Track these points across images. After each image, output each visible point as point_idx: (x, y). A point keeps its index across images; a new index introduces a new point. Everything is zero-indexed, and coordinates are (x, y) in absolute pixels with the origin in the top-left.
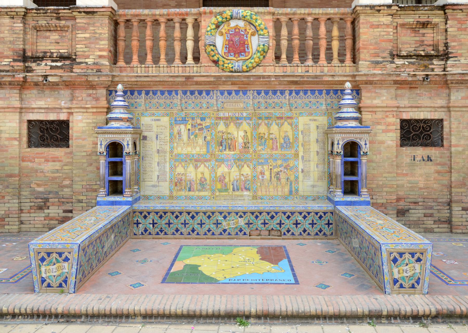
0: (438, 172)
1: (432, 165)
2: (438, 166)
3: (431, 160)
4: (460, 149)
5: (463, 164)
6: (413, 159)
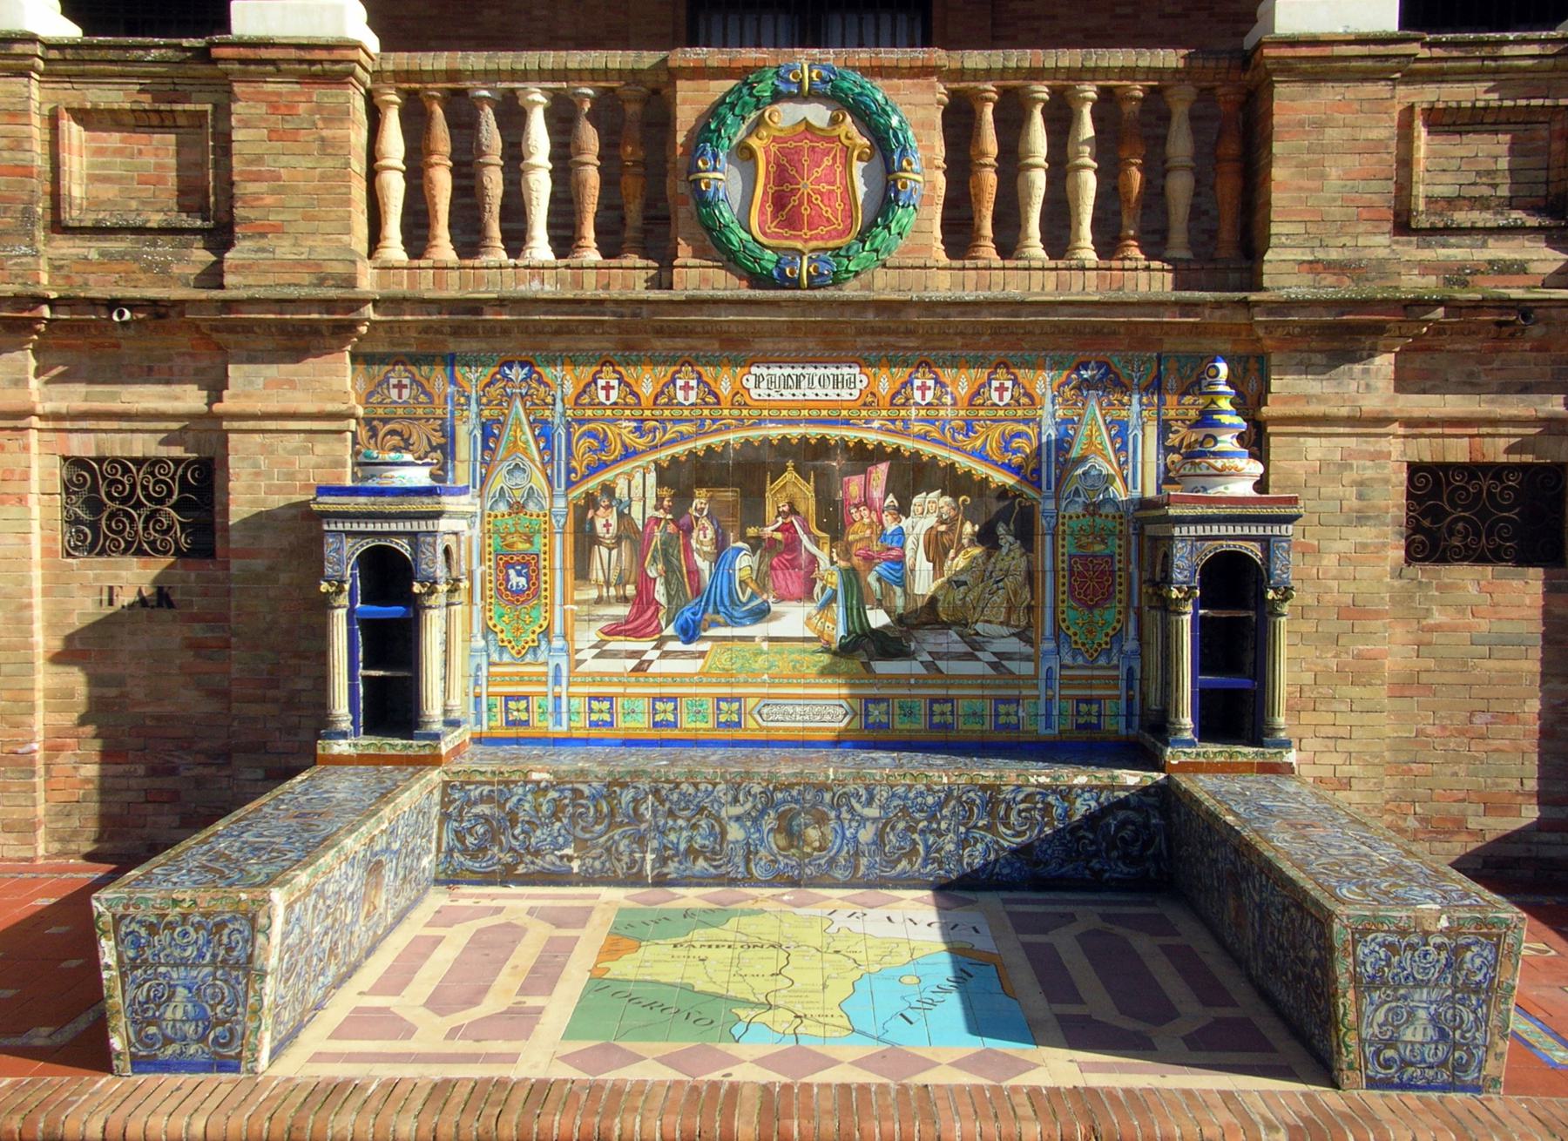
0: (196, 646)
1: (174, 620)
2: (197, 626)
3: (171, 605)
4: (259, 564)
5: (268, 618)
6: (105, 597)
